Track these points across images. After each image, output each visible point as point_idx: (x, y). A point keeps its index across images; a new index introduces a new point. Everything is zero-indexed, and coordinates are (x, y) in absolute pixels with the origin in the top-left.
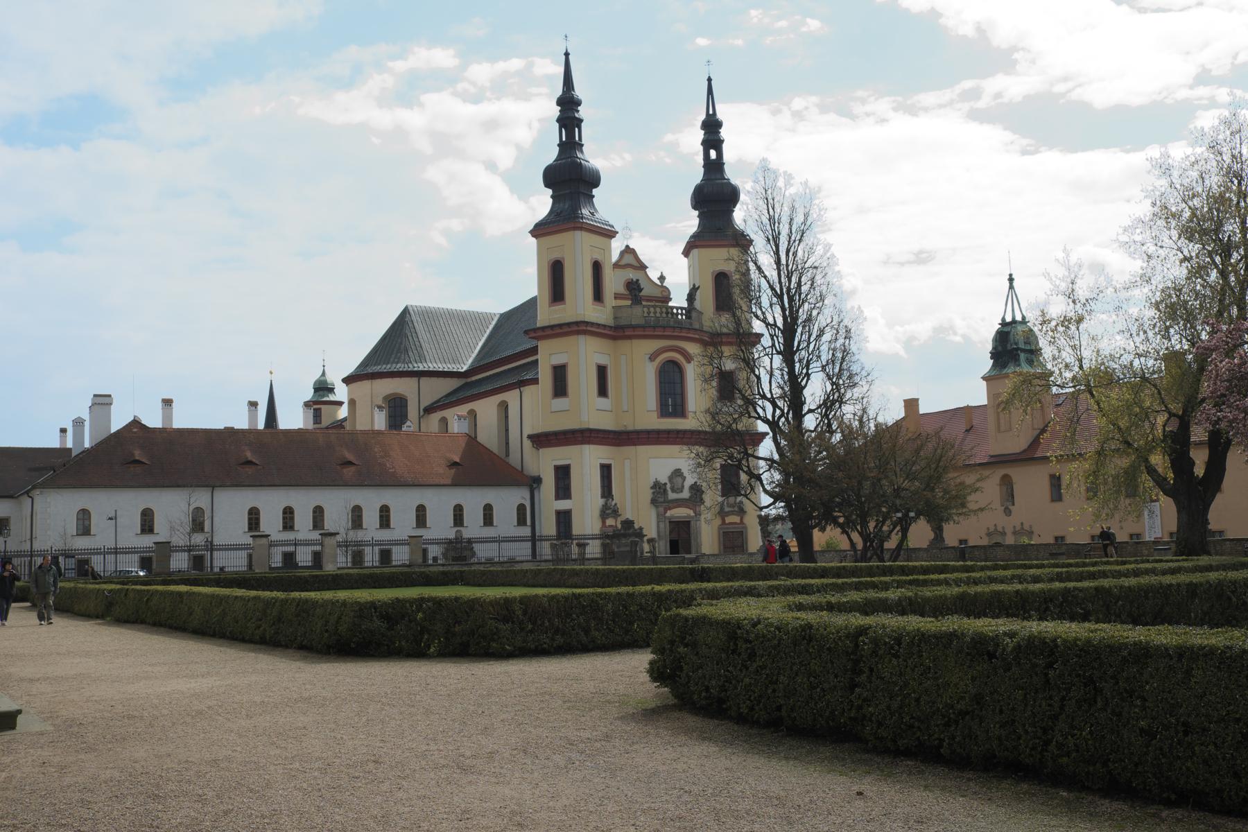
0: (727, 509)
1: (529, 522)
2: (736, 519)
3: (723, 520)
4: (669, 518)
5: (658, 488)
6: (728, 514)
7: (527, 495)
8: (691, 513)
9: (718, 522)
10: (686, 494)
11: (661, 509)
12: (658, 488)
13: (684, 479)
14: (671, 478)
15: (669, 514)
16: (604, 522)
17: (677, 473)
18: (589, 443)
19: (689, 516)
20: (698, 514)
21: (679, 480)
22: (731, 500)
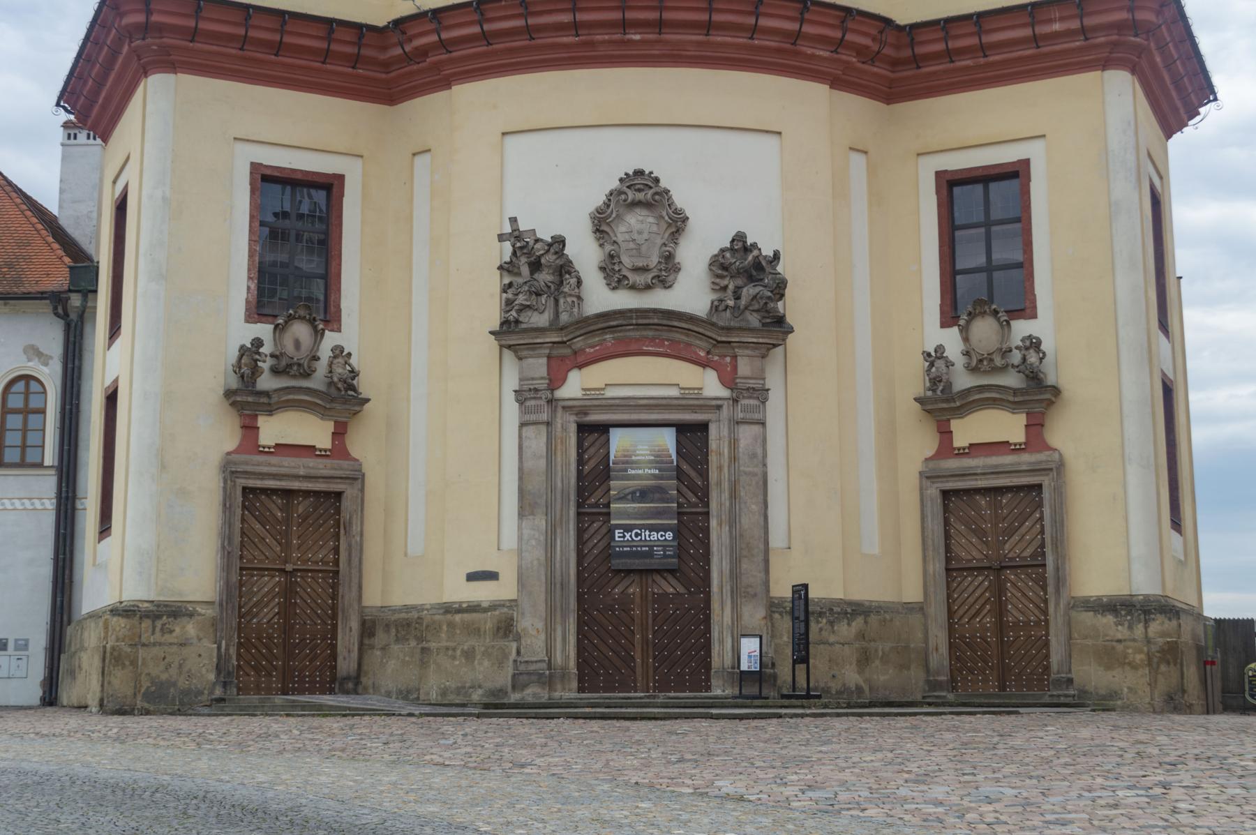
0: (963, 381)
1: (50, 457)
2: (1005, 426)
3: (945, 433)
4: (578, 409)
5: (535, 266)
6: (967, 403)
7: (51, 337)
8: (711, 385)
9: (919, 443)
10: (691, 293)
11: (538, 367)
12: (535, 266)
13: (677, 224)
14: (601, 224)
15: (575, 386)
16: (250, 429)
17: (641, 191)
18: (170, 63)
19: (692, 400)
20: (749, 395)
21: (636, 224)
22: (985, 330)
